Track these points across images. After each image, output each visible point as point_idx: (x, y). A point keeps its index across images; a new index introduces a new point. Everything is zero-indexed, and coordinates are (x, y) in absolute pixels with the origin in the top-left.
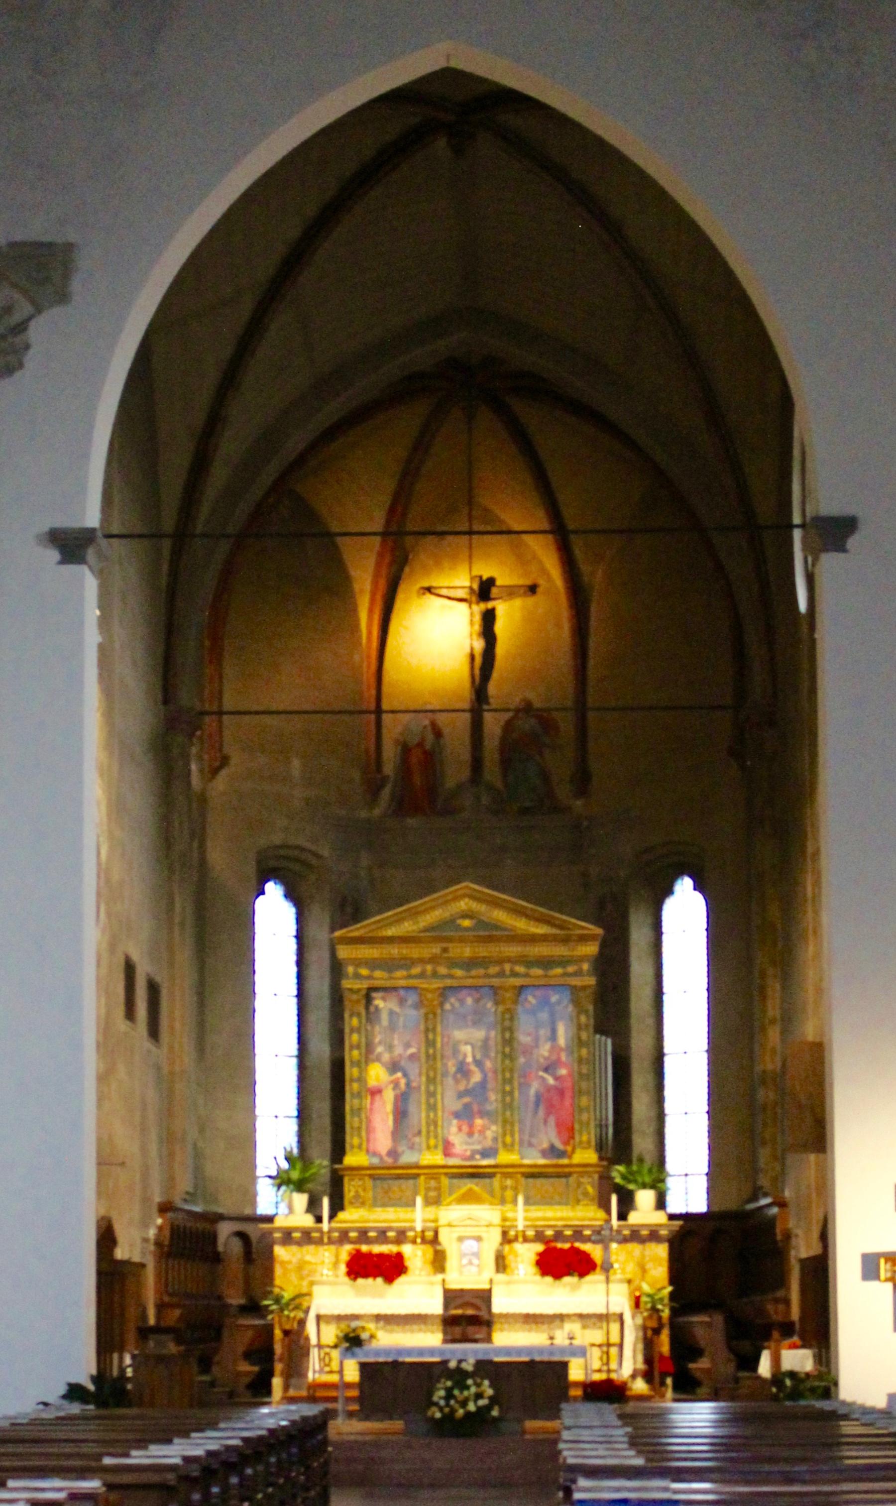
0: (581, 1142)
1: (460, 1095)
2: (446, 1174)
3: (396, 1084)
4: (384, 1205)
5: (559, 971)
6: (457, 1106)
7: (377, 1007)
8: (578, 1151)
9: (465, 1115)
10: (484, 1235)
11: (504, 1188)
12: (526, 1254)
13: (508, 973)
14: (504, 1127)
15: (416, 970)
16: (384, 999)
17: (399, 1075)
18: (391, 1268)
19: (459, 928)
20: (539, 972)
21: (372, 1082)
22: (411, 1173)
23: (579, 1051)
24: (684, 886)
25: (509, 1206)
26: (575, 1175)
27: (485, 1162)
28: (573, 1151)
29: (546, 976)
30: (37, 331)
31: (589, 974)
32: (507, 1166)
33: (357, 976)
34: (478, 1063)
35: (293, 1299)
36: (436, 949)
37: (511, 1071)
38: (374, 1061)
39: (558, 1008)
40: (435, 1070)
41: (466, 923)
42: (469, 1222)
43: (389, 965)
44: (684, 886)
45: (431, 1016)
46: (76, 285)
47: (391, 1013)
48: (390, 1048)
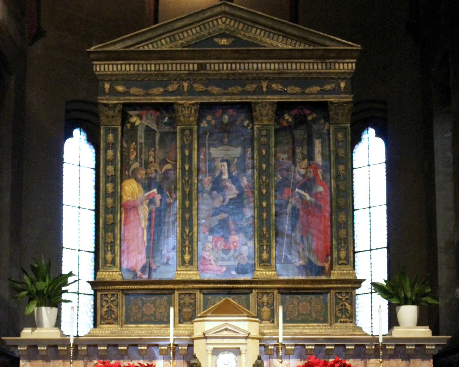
0: (339, 258)
1: (216, 212)
2: (201, 289)
3: (151, 202)
4: (137, 322)
5: (316, 89)
6: (215, 221)
7: (133, 124)
8: (336, 267)
10: (242, 347)
11: (260, 305)
13: (265, 89)
14: (260, 241)
15: (173, 87)
16: (140, 117)
17: (155, 190)
19: (217, 45)
20: (297, 89)
21: (126, 198)
22: (163, 290)
23: (337, 168)
25: (266, 324)
26: (333, 292)
27: (242, 278)
28: (331, 268)
29: (304, 93)
31: (346, 91)
32: (263, 282)
33: (113, 92)
34: (234, 180)
36: (193, 66)
37: (268, 186)
38: (129, 177)
39: (315, 127)
40: (191, 185)
41: (224, 41)
42: (225, 333)
43: (146, 82)
45: (187, 132)
47: (148, 130)
48: (147, 165)
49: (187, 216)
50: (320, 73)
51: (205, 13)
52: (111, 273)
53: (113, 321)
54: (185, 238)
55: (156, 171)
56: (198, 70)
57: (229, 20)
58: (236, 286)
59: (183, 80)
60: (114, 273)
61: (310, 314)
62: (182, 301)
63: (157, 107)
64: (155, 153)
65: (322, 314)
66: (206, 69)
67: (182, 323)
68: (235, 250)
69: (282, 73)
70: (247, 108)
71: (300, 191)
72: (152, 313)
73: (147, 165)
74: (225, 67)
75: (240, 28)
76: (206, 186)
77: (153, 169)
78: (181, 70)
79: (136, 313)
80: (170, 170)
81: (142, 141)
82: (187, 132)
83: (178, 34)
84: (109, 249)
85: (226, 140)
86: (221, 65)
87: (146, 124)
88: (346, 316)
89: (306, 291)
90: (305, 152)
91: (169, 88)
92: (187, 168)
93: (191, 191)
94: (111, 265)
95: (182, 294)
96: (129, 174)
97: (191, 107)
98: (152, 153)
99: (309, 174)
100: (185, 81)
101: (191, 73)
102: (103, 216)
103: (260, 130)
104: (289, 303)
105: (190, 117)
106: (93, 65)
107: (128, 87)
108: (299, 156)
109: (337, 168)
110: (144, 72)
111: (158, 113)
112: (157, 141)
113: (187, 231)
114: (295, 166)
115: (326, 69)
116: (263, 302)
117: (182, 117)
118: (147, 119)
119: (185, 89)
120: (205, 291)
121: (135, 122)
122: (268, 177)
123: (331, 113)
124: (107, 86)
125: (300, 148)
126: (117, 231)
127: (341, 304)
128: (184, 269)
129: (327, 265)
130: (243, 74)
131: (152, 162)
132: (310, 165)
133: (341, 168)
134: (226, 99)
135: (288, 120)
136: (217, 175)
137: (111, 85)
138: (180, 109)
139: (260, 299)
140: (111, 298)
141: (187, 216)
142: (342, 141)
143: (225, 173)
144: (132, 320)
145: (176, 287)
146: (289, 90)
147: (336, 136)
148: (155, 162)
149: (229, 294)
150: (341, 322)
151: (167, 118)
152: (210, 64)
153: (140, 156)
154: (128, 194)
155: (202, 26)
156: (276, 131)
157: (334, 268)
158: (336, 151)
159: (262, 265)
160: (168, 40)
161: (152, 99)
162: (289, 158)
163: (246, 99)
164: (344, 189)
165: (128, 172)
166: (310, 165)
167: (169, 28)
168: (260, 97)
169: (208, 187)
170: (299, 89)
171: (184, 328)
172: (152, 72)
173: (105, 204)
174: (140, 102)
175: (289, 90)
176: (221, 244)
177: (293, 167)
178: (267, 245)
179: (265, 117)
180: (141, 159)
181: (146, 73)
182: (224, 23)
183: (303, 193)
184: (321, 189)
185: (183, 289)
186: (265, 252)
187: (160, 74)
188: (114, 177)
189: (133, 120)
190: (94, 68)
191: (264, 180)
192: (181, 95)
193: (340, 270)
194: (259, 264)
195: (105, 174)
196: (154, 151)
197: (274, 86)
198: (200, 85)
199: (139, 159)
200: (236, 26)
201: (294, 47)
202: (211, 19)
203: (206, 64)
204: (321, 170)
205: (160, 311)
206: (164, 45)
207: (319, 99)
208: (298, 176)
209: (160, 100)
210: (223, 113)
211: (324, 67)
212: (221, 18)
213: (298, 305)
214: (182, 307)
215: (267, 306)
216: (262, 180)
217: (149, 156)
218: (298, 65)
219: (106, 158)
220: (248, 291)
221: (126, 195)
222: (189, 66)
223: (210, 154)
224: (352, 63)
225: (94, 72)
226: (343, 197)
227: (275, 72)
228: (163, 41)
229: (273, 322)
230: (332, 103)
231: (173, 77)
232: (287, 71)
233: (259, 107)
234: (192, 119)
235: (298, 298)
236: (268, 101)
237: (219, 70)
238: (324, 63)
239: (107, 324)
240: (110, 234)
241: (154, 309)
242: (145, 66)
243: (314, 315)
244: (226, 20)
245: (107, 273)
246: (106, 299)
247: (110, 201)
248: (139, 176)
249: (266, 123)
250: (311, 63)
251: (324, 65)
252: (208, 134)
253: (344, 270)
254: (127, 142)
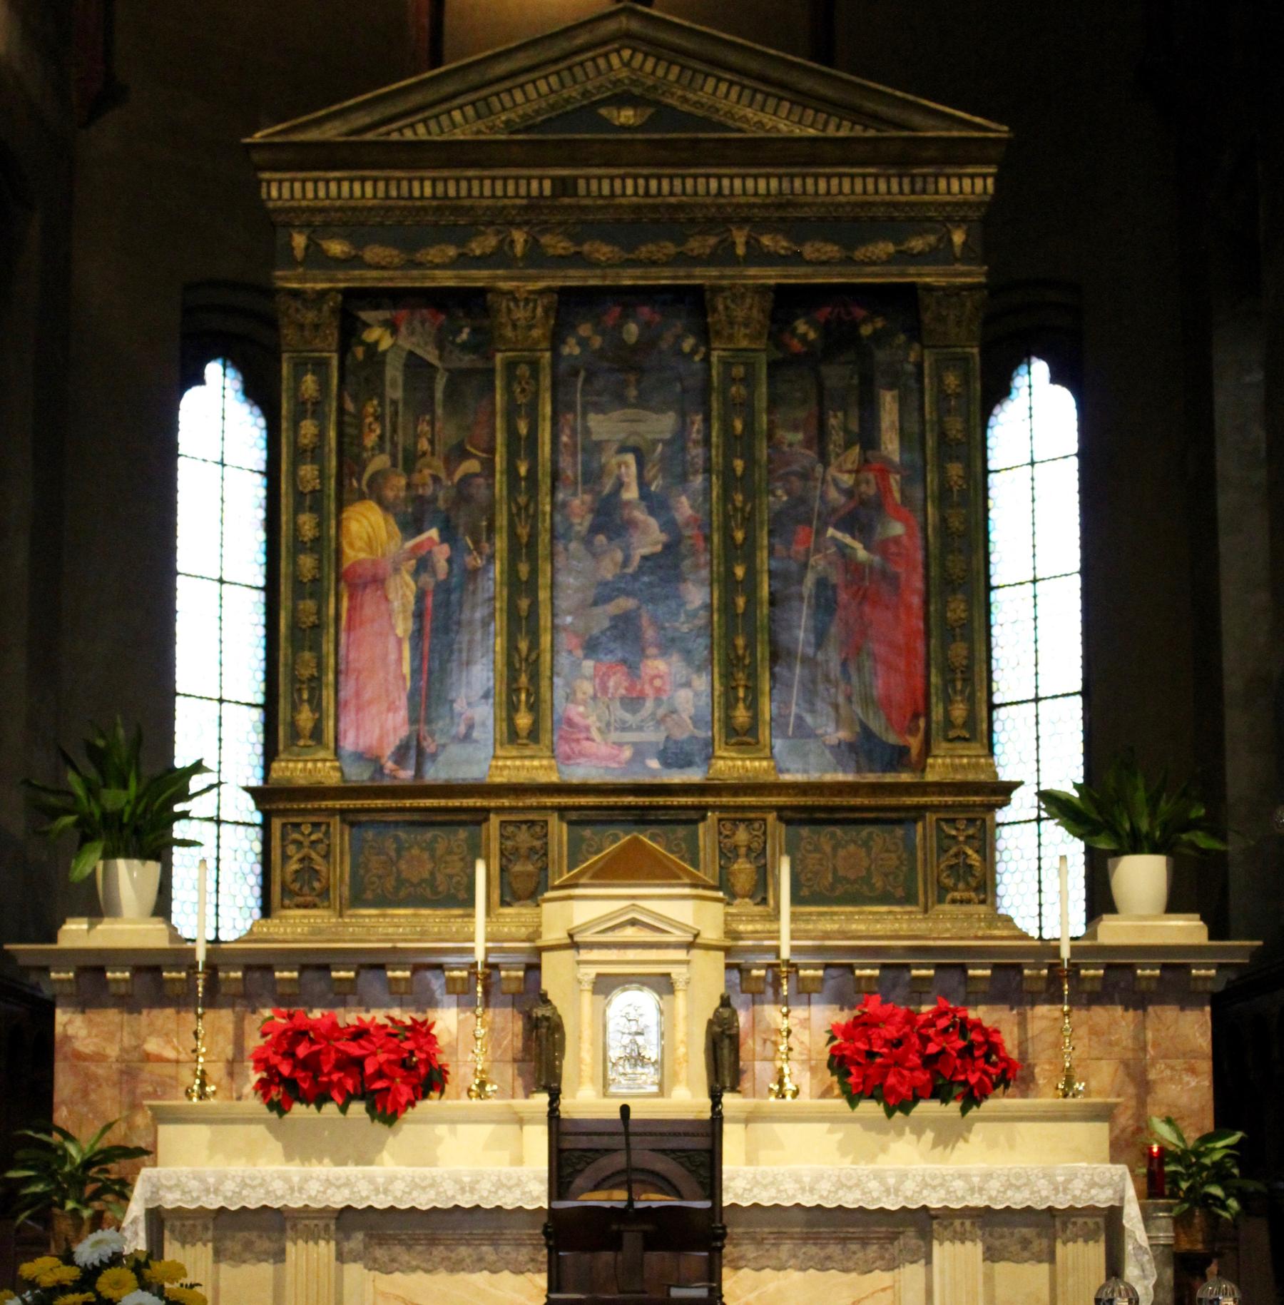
0: (948, 723)
1: (605, 594)
2: (561, 810)
3: (423, 564)
4: (383, 902)
5: (884, 248)
6: (601, 618)
7: (372, 348)
8: (940, 747)
10: (677, 972)
11: (728, 854)
12: (801, 1032)
13: (740, 250)
14: (727, 676)
15: (483, 244)
16: (392, 326)
17: (433, 533)
18: (397, 1078)
19: (608, 126)
20: (832, 250)
21: (354, 554)
22: (457, 812)
23: (942, 470)
25: (745, 906)
26: (931, 817)
27: (677, 777)
28: (926, 750)
29: (849, 261)
31: (968, 255)
32: (737, 789)
33: (317, 259)
34: (656, 504)
35: (88, 1164)
36: (540, 184)
37: (749, 522)
38: (362, 497)
39: (881, 356)
40: (534, 518)
41: (627, 116)
42: (630, 934)
43: (409, 229)
45: (523, 370)
47: (415, 365)
48: (410, 461)
49: (524, 604)
50: (895, 205)
51: (575, 38)
52: (310, 765)
53: (317, 900)
54: (517, 666)
55: (436, 479)
56: (554, 195)
57: (640, 57)
58: (661, 800)
59: (511, 224)
60: (319, 765)
61: (867, 880)
62: (509, 843)
63: (439, 299)
64: (433, 429)
65: (902, 878)
66: (575, 195)
67: (509, 905)
68: (658, 700)
69: (790, 204)
70: (692, 303)
71: (839, 535)
72: (426, 875)
73: (410, 461)
74: (629, 188)
75: (672, 77)
76: (576, 520)
77: (427, 472)
78: (505, 196)
79: (380, 877)
80: (476, 475)
81: (398, 394)
82: (523, 370)
83: (497, 94)
84: (305, 696)
85: (632, 393)
86: (618, 183)
87: (408, 347)
88: (967, 884)
89: (857, 815)
90: (854, 426)
91: (473, 245)
92: (523, 470)
93: (533, 536)
94: (310, 743)
95: (510, 822)
96: (360, 489)
97: (535, 301)
98: (424, 427)
99: (863, 488)
100: (519, 226)
101: (534, 205)
102: (289, 604)
103: (726, 364)
104: (809, 847)
105: (530, 327)
106: (260, 182)
107: (359, 243)
108: (837, 437)
109: (942, 470)
110: (402, 203)
111: (443, 317)
112: (439, 395)
113: (523, 646)
114: (826, 464)
115: (913, 192)
116: (736, 847)
117: (509, 328)
118: (412, 333)
119: (519, 249)
120: (574, 816)
121: (377, 343)
122: (751, 496)
123: (927, 317)
124: (299, 241)
125: (840, 414)
126: (328, 647)
127: (953, 850)
128: (514, 753)
129: (914, 743)
130: (680, 207)
131: (424, 454)
132: (866, 461)
133: (955, 470)
134: (631, 278)
135: (805, 335)
136: (607, 489)
137: (309, 238)
138: (504, 305)
139: (727, 836)
140: (310, 834)
141: (524, 604)
142: (958, 396)
143: (629, 484)
144: (369, 895)
145: (493, 803)
146: (808, 251)
147: (940, 380)
148: (433, 454)
149: (640, 825)
150: (954, 901)
151: (466, 331)
152: (588, 179)
153: (392, 438)
154: (359, 544)
155: (565, 74)
156: (773, 366)
157: (935, 752)
158: (940, 422)
159: (733, 741)
160: (470, 111)
161: (424, 278)
162: (808, 444)
163: (688, 277)
164: (962, 528)
165: (359, 481)
166: (866, 461)
167: (474, 78)
168: (728, 271)
169: (581, 524)
170: (836, 248)
171: (516, 917)
172: (425, 203)
173: (294, 571)
174: (391, 285)
175: (808, 251)
176: (618, 683)
177: (819, 468)
178: (746, 687)
179: (742, 331)
180: (394, 445)
181: (409, 203)
182: (627, 64)
183: (848, 539)
184: (897, 529)
185: (511, 809)
186: (741, 705)
187: (446, 206)
188: (318, 495)
189: (373, 335)
190: (264, 190)
191: (739, 504)
192: (508, 267)
193: (951, 756)
194: (723, 739)
195: (295, 486)
196: (432, 424)
197: (766, 240)
198: (560, 237)
199: (388, 446)
200: (660, 72)
201: (824, 130)
202: (590, 54)
203: (575, 178)
204: (898, 477)
205: (448, 871)
206: (460, 125)
207: (893, 277)
208: (833, 494)
209: (446, 279)
210: (625, 317)
211: (906, 188)
212: (618, 51)
213: (835, 856)
214: (510, 860)
215: (747, 856)
216: (734, 505)
217: (417, 437)
218: (835, 182)
219: (295, 442)
220: (693, 815)
221: (351, 545)
222: (529, 185)
223: (587, 431)
224: (985, 176)
225: (263, 201)
226: (960, 551)
227: (768, 201)
228: (457, 115)
229: (764, 901)
230: (929, 288)
231: (484, 214)
232: (803, 199)
233: (725, 298)
234: (536, 333)
235: (833, 835)
236: (751, 282)
237: (613, 195)
238: (907, 175)
239: (298, 906)
240: (307, 655)
241: (429, 866)
242: (405, 184)
243: (878, 882)
244: (632, 57)
245: (300, 765)
246: (296, 836)
247: (307, 562)
248: (390, 494)
249: (744, 344)
250: (870, 175)
251: (906, 181)
252: (582, 374)
253: (961, 756)
254: (355, 398)
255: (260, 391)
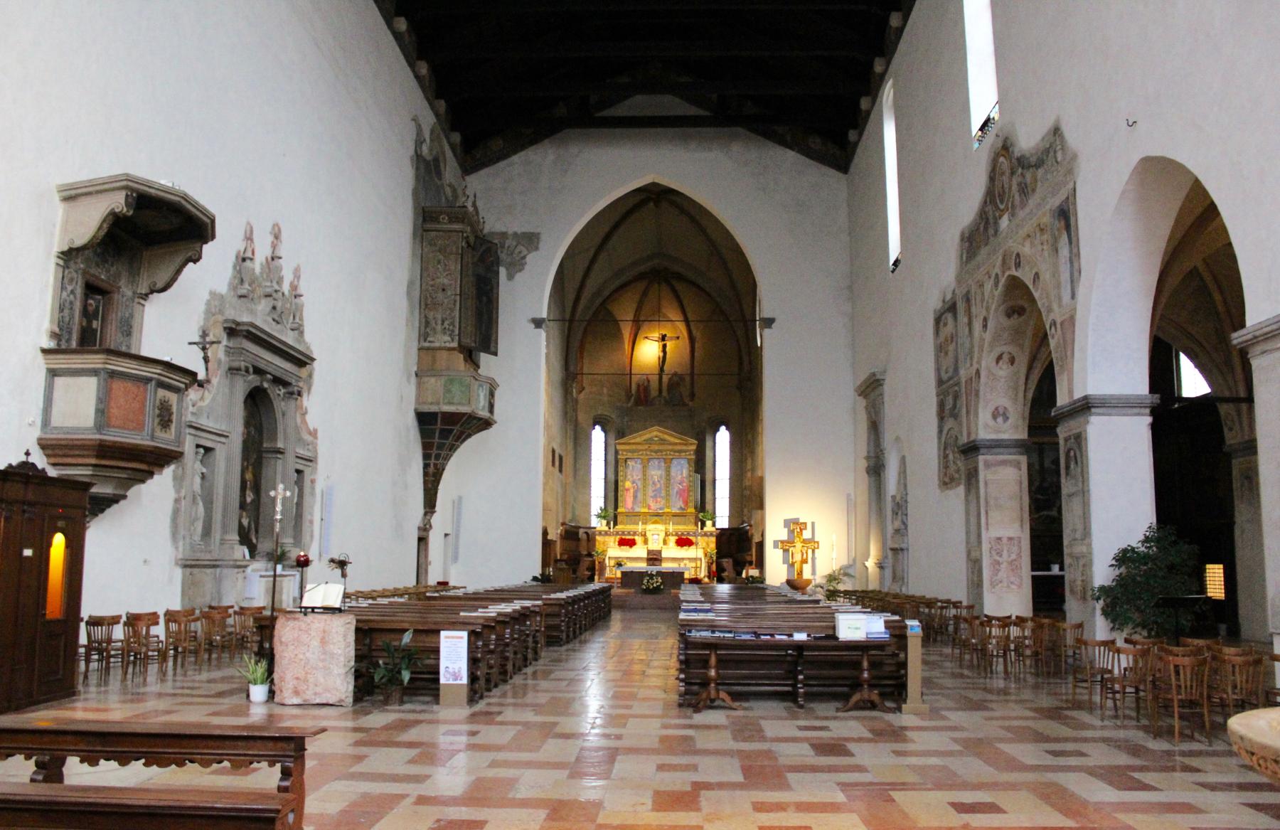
9: (655, 497)
12: (673, 539)
18: (631, 543)
22: (637, 515)
24: (723, 428)
30: (528, 259)
43: (633, 451)
44: (723, 428)
46: (541, 245)
149: (658, 516)
255: (604, 430)
